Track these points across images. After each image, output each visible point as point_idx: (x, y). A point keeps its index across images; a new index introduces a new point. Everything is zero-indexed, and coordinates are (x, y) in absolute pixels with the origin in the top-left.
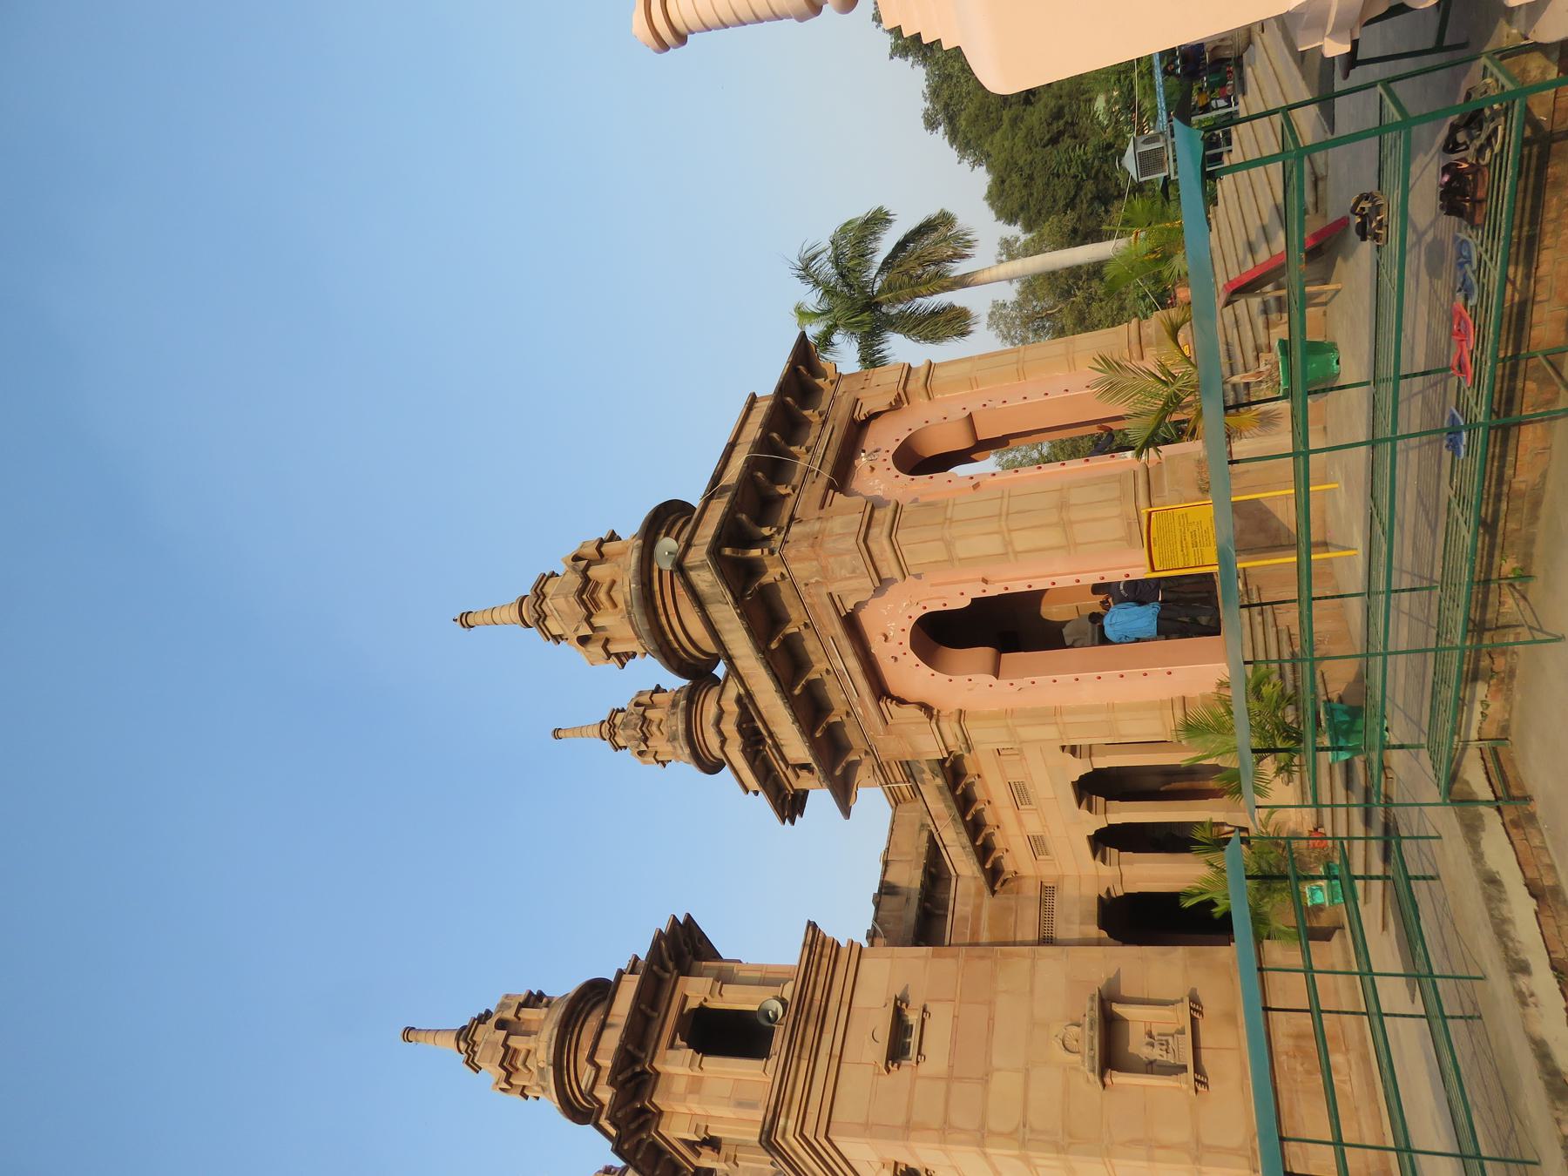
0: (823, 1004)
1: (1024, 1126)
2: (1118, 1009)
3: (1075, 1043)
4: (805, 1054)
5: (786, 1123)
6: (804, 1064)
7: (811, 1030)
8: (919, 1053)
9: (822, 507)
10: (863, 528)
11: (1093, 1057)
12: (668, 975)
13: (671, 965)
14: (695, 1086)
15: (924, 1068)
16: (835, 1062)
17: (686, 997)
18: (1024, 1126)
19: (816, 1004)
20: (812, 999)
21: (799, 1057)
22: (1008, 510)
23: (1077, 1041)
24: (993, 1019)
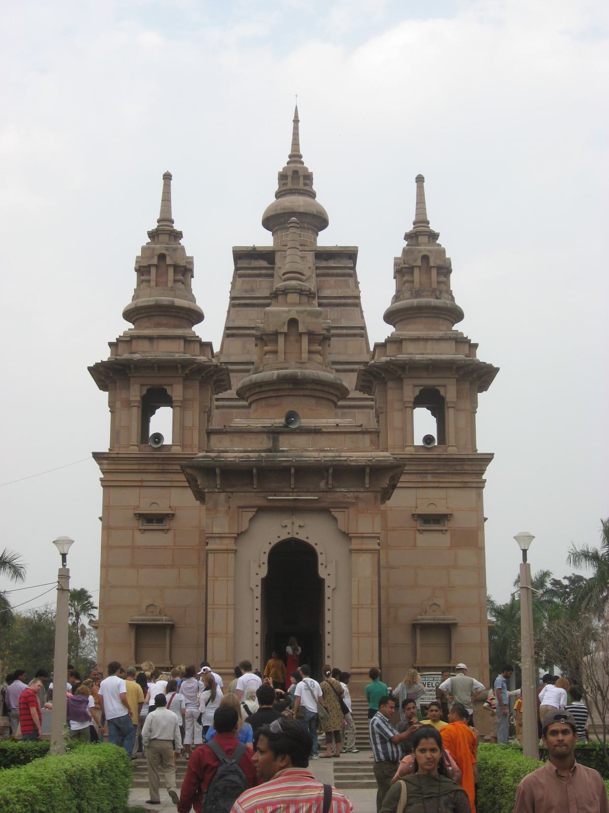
0: (171, 471)
1: (111, 587)
2: (168, 632)
3: (152, 610)
4: (142, 467)
5: (105, 464)
6: (136, 467)
7: (155, 467)
8: (145, 530)
9: (239, 507)
10: (217, 535)
11: (138, 621)
12: (180, 372)
13: (187, 371)
15: (138, 534)
16: (139, 484)
17: (171, 385)
18: (111, 587)
19: (170, 467)
20: (172, 464)
21: (139, 464)
22: (216, 608)
23: (152, 612)
24: (164, 568)
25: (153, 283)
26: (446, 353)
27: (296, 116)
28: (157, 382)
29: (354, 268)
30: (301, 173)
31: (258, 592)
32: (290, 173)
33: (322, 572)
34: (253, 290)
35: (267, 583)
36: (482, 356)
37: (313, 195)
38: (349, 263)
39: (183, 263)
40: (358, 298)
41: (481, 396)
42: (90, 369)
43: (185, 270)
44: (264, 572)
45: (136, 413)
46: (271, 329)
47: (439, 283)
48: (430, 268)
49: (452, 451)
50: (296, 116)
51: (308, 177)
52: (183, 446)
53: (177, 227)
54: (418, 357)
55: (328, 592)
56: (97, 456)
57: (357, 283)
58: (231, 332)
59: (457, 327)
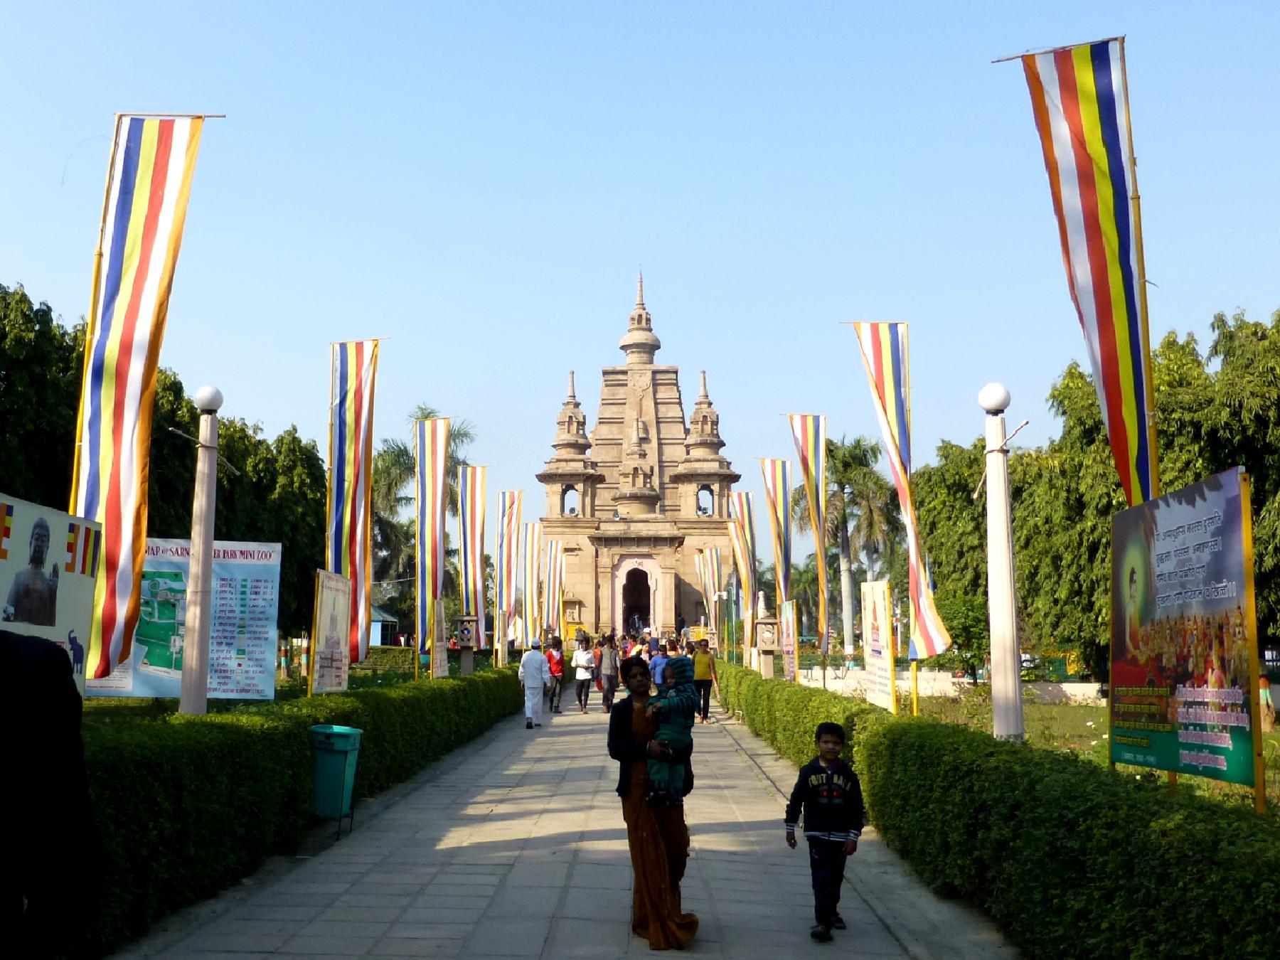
14: (554, 493)
25: (566, 430)
26: (713, 467)
27: (641, 278)
28: (569, 483)
29: (676, 379)
30: (644, 317)
31: (622, 591)
32: (636, 318)
33: (650, 582)
34: (614, 395)
35: (626, 588)
36: (735, 469)
37: (650, 330)
38: (674, 376)
39: (581, 420)
40: (680, 398)
41: (733, 485)
42: (537, 476)
43: (582, 424)
44: (624, 581)
45: (558, 497)
46: (627, 472)
47: (712, 429)
48: (706, 424)
49: (716, 517)
50: (641, 278)
51: (648, 320)
52: (584, 515)
53: (578, 399)
54: (699, 471)
55: (652, 592)
56: (541, 520)
57: (678, 387)
58: (602, 421)
59: (722, 451)
